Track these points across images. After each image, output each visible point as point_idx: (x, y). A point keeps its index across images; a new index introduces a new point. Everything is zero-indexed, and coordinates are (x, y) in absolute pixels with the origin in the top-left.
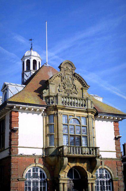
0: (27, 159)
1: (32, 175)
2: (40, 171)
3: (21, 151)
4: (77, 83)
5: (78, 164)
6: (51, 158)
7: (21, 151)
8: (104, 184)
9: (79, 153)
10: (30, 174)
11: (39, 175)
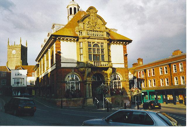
0: (67, 70)
2: (76, 77)
3: (63, 65)
4: (99, 20)
6: (81, 69)
8: (116, 83)
9: (98, 65)
11: (75, 79)
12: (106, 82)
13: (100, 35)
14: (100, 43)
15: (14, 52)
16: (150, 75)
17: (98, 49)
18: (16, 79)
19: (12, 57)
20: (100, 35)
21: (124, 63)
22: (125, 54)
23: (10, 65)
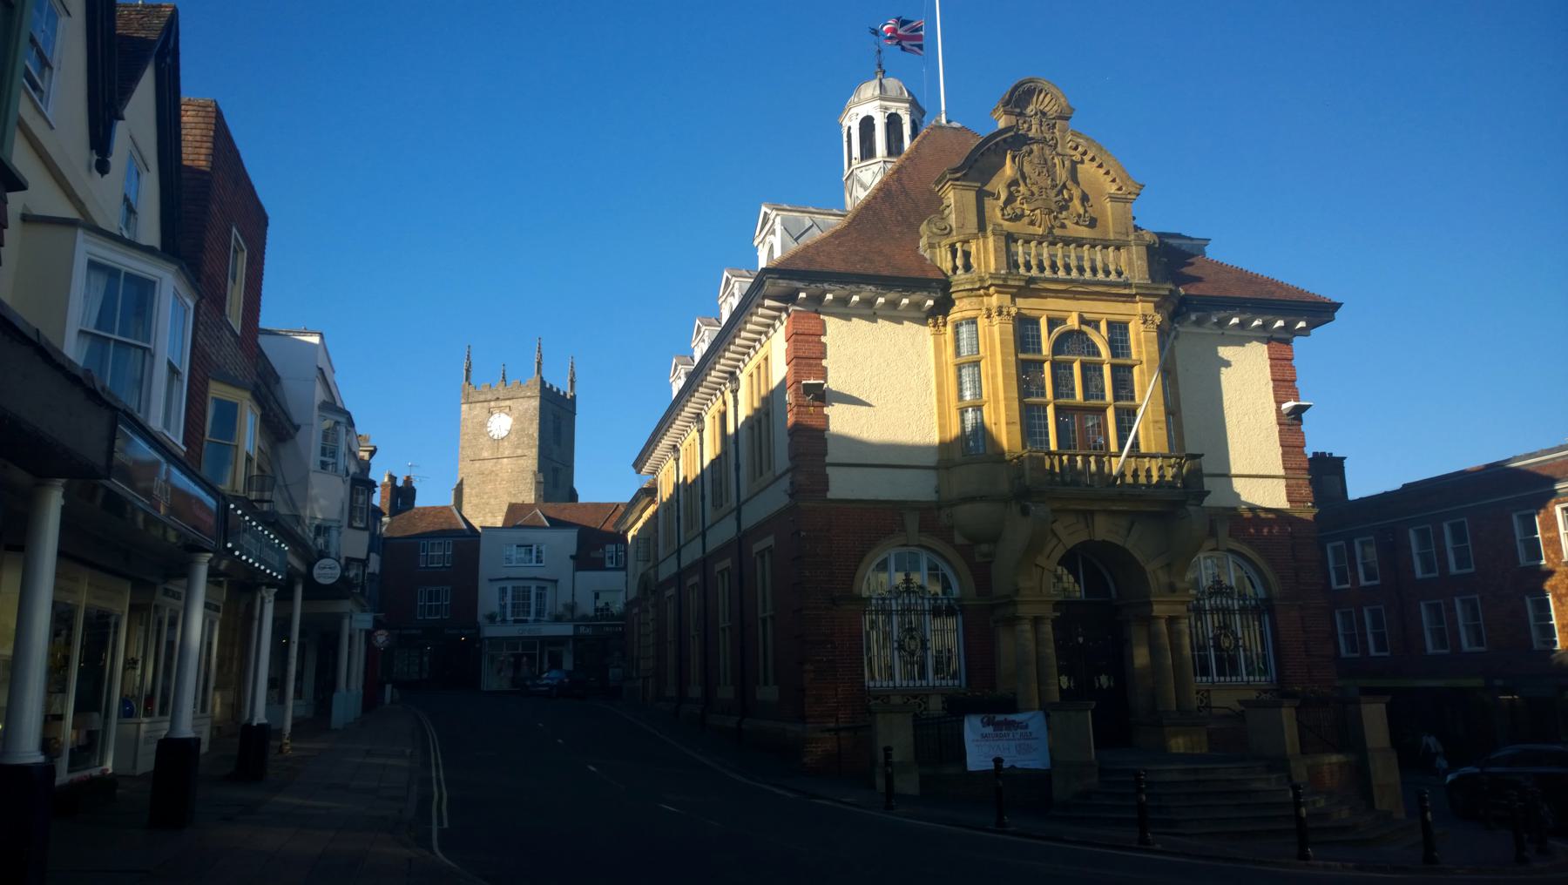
3: (842, 486)
13: (1087, 265)
14: (1103, 326)
16: (1428, 567)
17: (1091, 371)
18: (509, 586)
19: (485, 454)
20: (1087, 265)
21: (1282, 472)
22: (1287, 406)
23: (475, 501)
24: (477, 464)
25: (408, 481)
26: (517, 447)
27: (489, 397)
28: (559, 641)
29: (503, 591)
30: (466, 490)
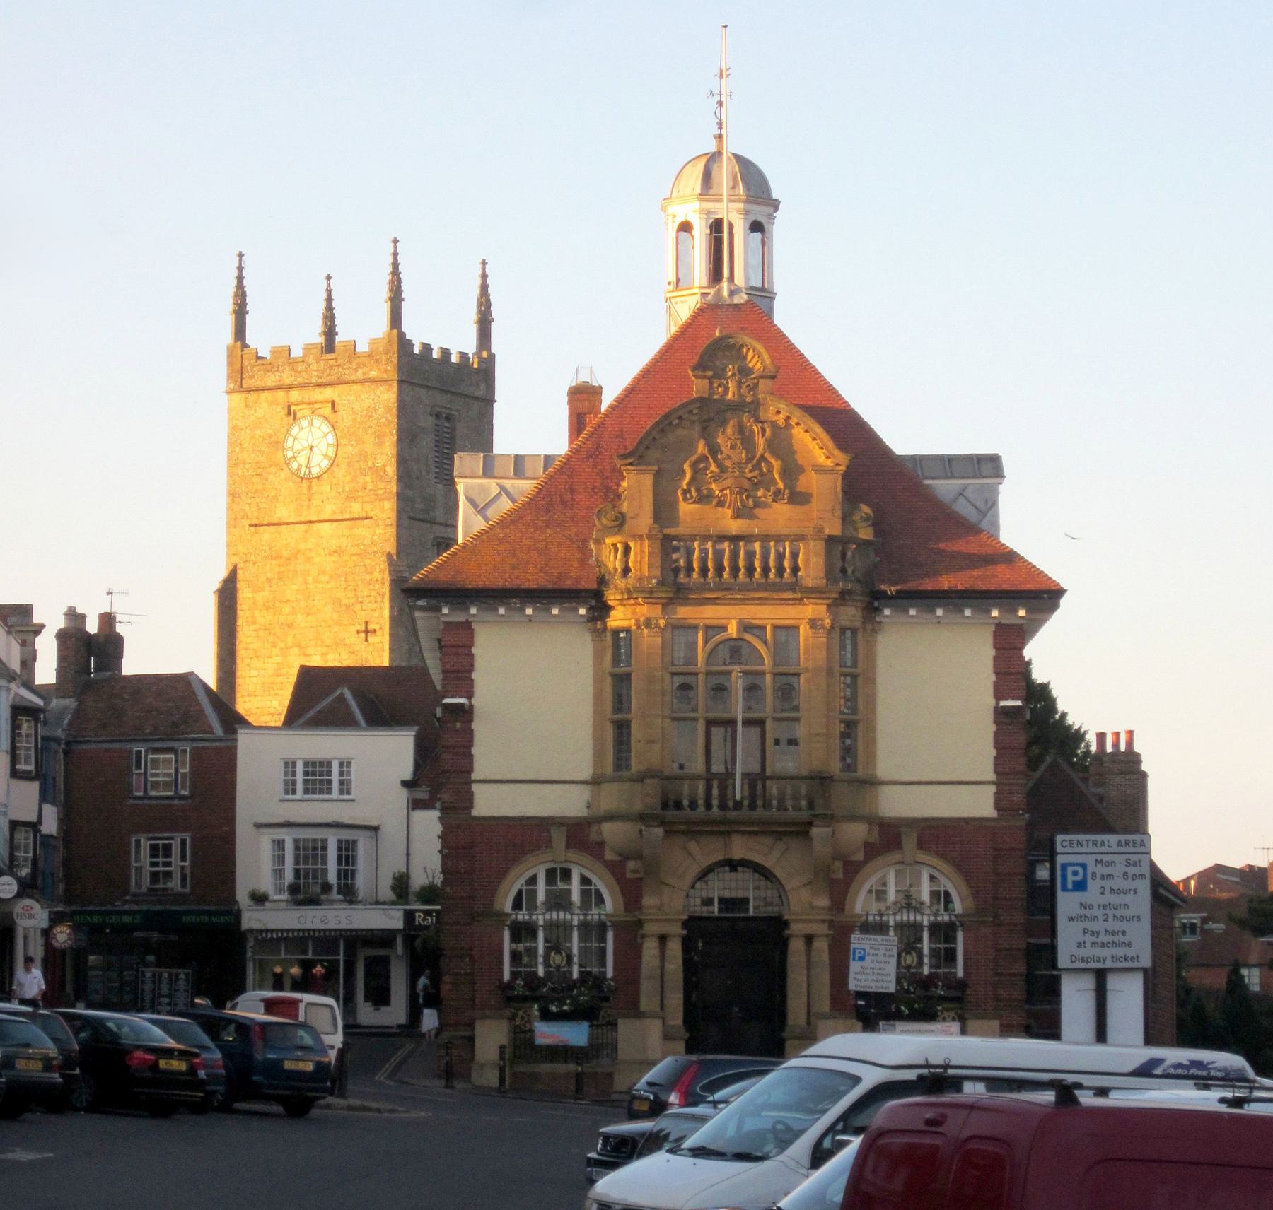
1: (541, 896)
2: (585, 881)
5: (740, 849)
7: (488, 802)
10: (533, 894)
11: (576, 897)
12: (795, 928)
15: (312, 441)
19: (283, 512)
21: (992, 777)
23: (263, 618)
24: (267, 534)
25: (108, 620)
26: (350, 498)
27: (288, 380)
28: (383, 939)
29: (279, 844)
30: (244, 594)
